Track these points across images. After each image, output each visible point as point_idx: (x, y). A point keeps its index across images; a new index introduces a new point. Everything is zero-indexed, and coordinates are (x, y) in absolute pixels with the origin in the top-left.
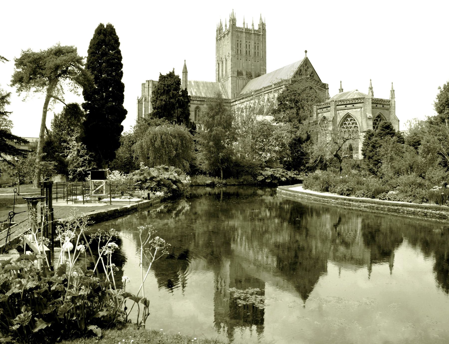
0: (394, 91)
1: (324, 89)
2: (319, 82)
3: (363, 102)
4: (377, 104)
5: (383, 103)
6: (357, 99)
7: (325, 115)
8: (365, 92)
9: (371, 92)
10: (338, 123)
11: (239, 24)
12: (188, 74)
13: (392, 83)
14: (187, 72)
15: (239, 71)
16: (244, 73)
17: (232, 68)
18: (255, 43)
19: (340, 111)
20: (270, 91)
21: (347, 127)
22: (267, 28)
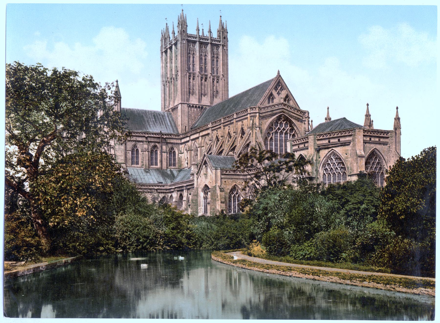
7: (303, 153)
8: (360, 121)
13: (397, 108)
18: (213, 57)
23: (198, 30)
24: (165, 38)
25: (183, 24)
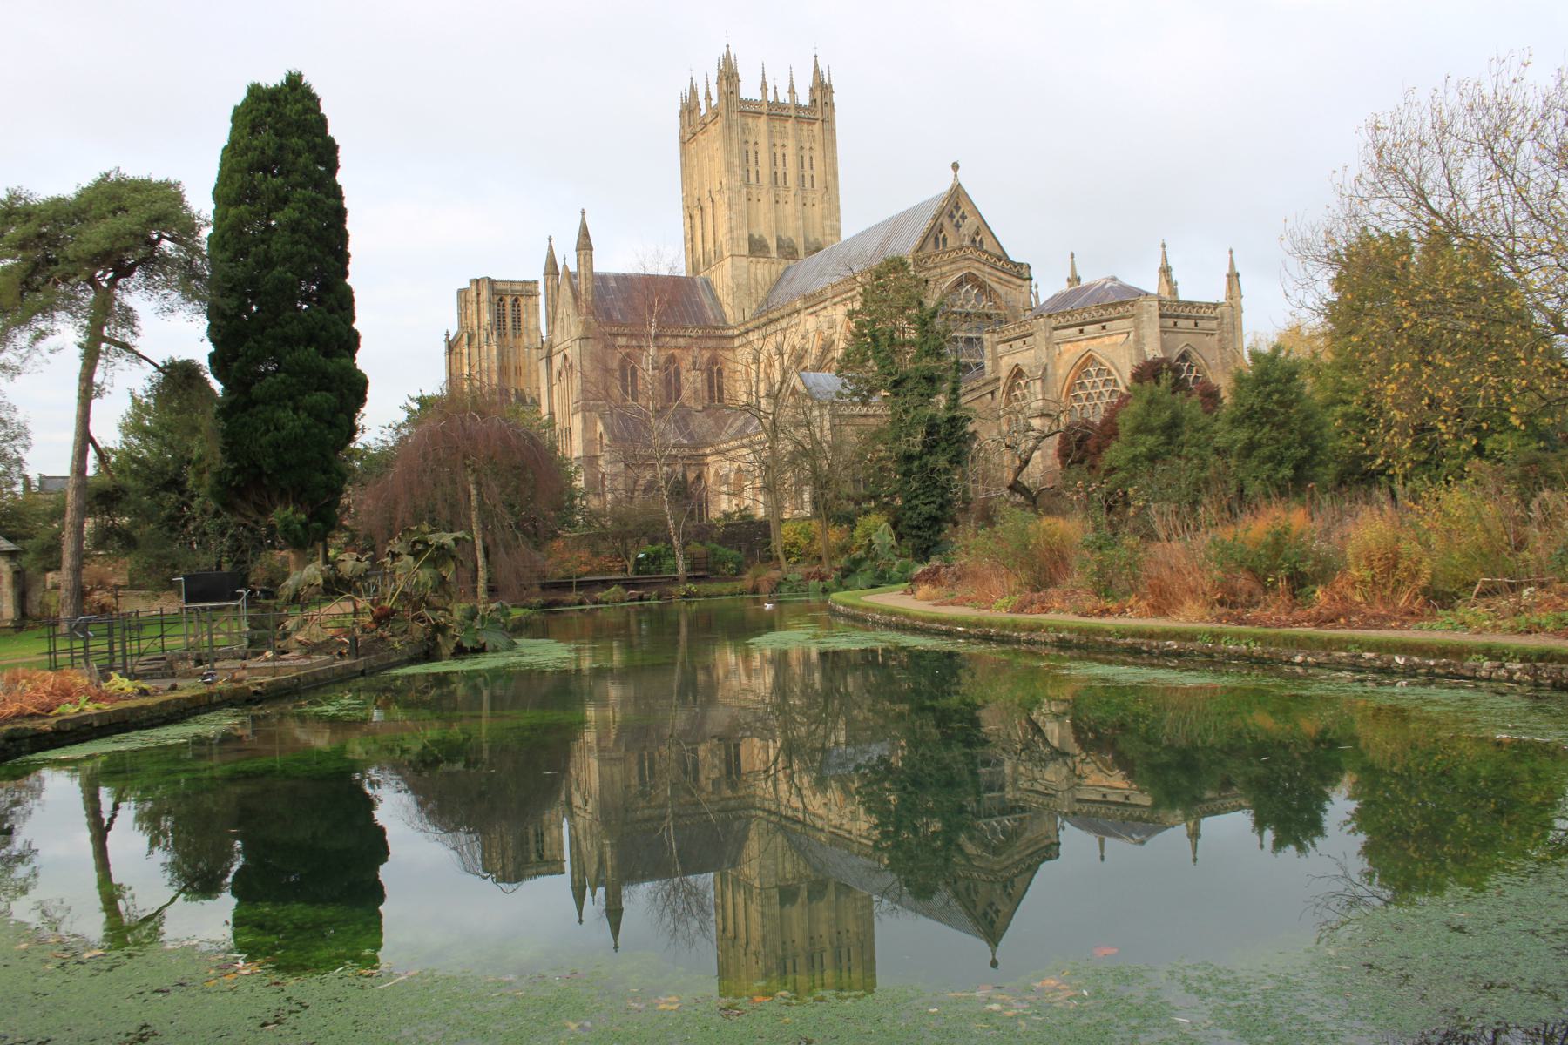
0: (1238, 275)
1: (1019, 282)
2: (1000, 260)
3: (1133, 316)
4: (1178, 317)
5: (1194, 314)
6: (1114, 306)
8: (1149, 282)
9: (1168, 281)
10: (1060, 385)
11: (749, 90)
12: (594, 253)
14: (591, 249)
15: (757, 237)
16: (772, 244)
17: (731, 230)
18: (802, 148)
19: (1063, 348)
20: (850, 294)
21: (1089, 396)
22: (837, 98)
23: (764, 87)
24: (689, 108)
25: (729, 76)
